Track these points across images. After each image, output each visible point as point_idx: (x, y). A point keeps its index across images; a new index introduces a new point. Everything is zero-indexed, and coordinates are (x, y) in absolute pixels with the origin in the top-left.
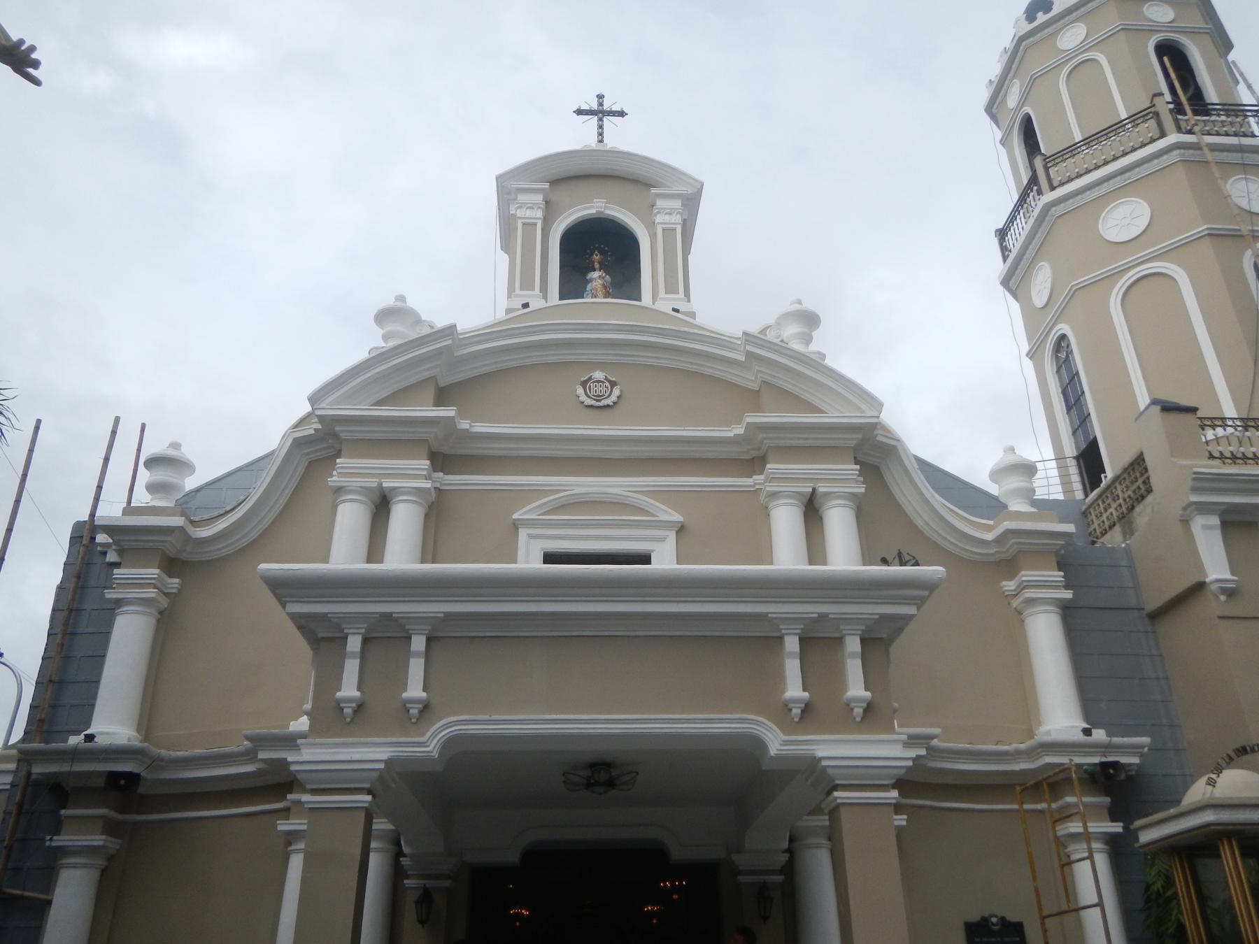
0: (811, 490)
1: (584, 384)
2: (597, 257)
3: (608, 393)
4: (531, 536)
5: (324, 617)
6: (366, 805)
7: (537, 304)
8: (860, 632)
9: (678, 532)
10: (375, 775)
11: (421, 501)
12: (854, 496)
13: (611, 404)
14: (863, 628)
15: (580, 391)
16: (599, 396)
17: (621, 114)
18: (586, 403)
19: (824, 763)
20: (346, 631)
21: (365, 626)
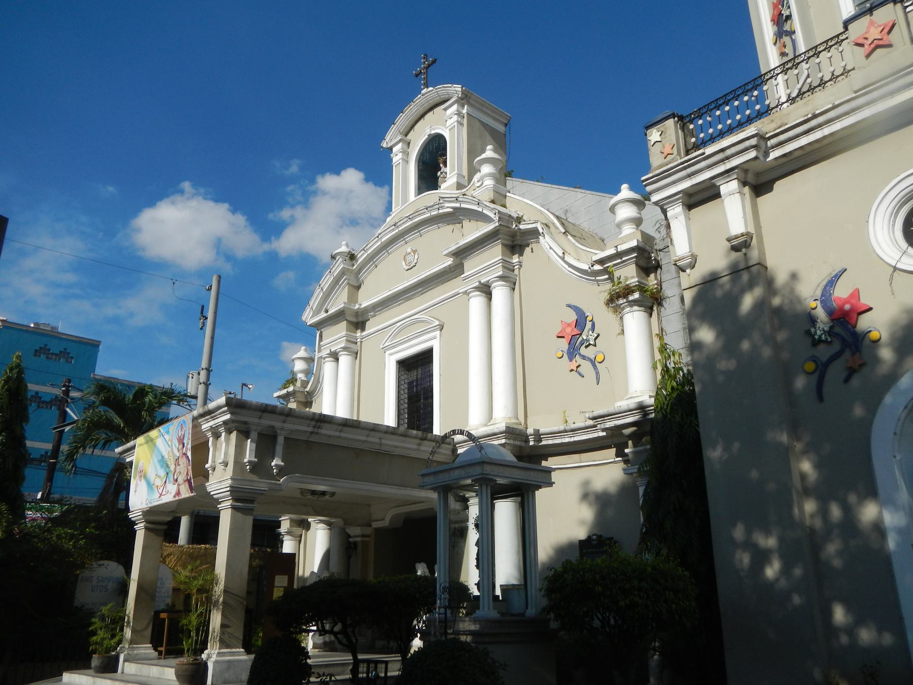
4: (391, 354)
9: (441, 330)
11: (347, 353)
12: (501, 278)
13: (414, 265)
15: (404, 263)
16: (410, 262)
19: (212, 493)
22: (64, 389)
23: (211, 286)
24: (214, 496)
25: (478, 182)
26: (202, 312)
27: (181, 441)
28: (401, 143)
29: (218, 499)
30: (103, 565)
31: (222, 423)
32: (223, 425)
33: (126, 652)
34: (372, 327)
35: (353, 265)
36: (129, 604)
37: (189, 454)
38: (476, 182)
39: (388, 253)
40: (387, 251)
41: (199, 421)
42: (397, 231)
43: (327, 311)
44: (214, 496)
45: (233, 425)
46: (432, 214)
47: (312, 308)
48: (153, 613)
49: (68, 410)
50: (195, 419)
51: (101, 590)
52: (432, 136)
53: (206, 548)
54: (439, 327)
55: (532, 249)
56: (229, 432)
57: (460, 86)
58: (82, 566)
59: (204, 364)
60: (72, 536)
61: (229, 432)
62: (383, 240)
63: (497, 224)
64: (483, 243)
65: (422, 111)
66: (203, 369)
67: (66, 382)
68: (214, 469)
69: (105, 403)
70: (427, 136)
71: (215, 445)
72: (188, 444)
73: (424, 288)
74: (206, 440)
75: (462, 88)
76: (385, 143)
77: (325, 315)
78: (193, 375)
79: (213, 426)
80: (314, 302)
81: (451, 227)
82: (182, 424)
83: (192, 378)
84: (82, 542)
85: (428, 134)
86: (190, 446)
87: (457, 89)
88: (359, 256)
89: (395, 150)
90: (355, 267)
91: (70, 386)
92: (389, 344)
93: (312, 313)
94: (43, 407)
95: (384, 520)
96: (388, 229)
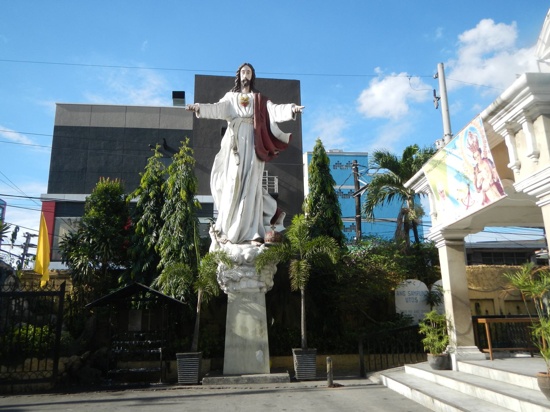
19: (525, 191)
22: (354, 167)
23: (437, 74)
24: (529, 193)
26: (435, 95)
27: (476, 148)
29: (534, 196)
30: (411, 282)
31: (522, 110)
32: (523, 114)
33: (456, 353)
36: (448, 311)
37: (490, 156)
41: (489, 122)
45: (537, 109)
48: (471, 319)
49: (359, 180)
50: (485, 120)
51: (413, 301)
53: (483, 268)
56: (532, 120)
58: (395, 284)
59: (446, 131)
60: (385, 261)
61: (532, 120)
66: (446, 135)
67: (354, 163)
68: (519, 167)
69: (384, 166)
71: (514, 143)
72: (485, 147)
74: (502, 140)
78: (439, 142)
82: (470, 132)
83: (439, 144)
84: (393, 264)
86: (488, 149)
91: (357, 165)
94: (345, 198)
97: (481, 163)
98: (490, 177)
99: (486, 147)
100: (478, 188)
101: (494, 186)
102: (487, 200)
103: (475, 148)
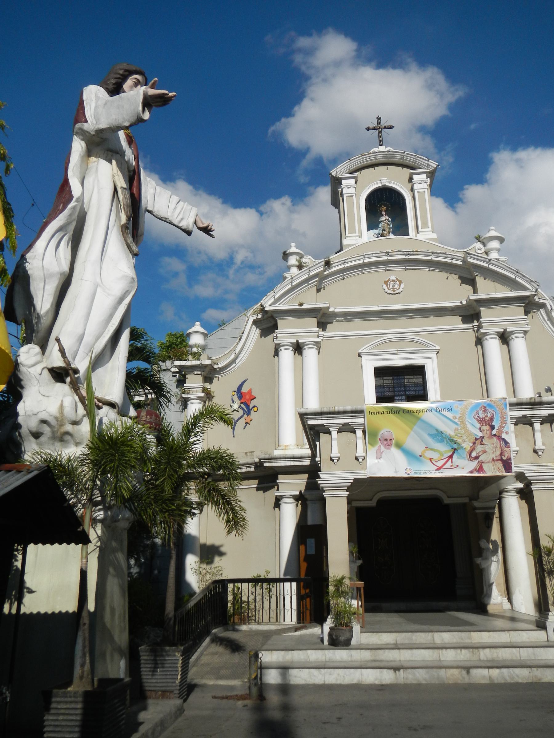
0: (503, 330)
1: (386, 283)
2: (385, 208)
3: (398, 288)
4: (368, 360)
5: (322, 425)
6: (347, 495)
7: (360, 242)
8: (540, 421)
9: (437, 354)
10: (350, 484)
11: (315, 347)
13: (400, 292)
14: (541, 419)
15: (385, 287)
16: (394, 289)
17: (391, 127)
18: (388, 293)
19: (526, 475)
20: (331, 430)
21: (338, 428)
24: (528, 477)
25: (479, 249)
28: (354, 180)
34: (333, 330)
35: (325, 271)
38: (477, 248)
39: (362, 272)
40: (362, 271)
42: (385, 258)
43: (301, 305)
44: (528, 477)
46: (433, 259)
47: (274, 296)
52: (384, 187)
54: (438, 351)
55: (532, 316)
57: (437, 164)
62: (366, 261)
63: (534, 293)
64: (509, 301)
65: (378, 161)
70: (380, 185)
73: (415, 314)
75: (438, 166)
76: (335, 172)
77: (298, 307)
79: (527, 416)
80: (280, 291)
81: (445, 275)
85: (383, 184)
87: (430, 163)
88: (334, 265)
89: (344, 182)
90: (326, 273)
92: (368, 351)
93: (273, 300)
95: (371, 500)
96: (376, 253)
97: (488, 437)
98: (498, 453)
99: (504, 427)
100: (472, 457)
101: (500, 462)
102: (480, 469)
103: (485, 422)
